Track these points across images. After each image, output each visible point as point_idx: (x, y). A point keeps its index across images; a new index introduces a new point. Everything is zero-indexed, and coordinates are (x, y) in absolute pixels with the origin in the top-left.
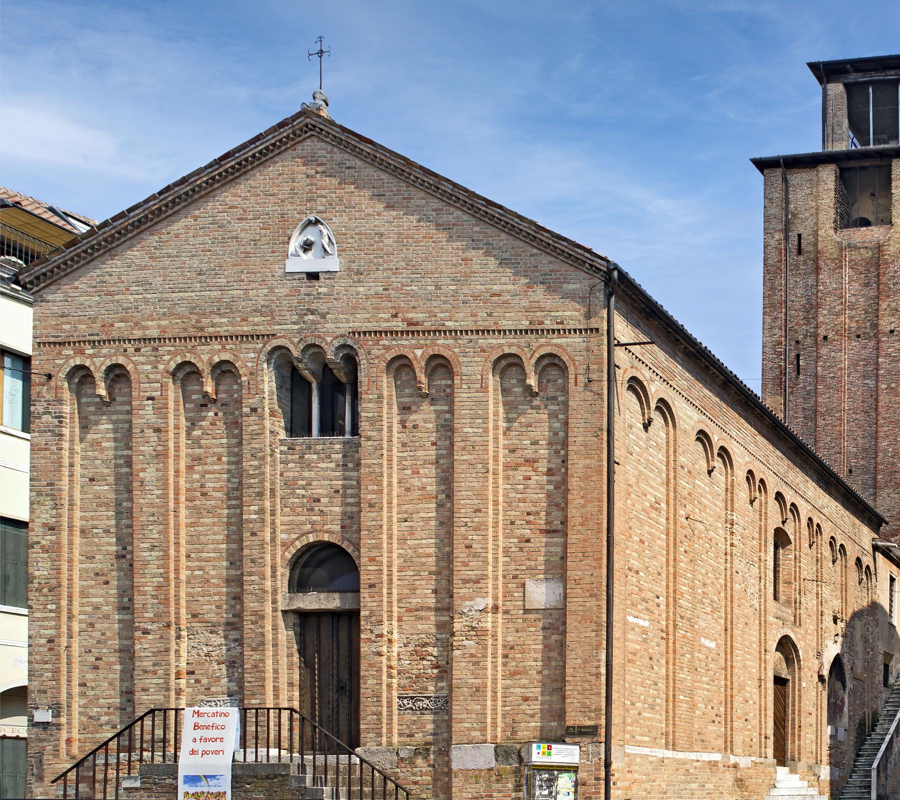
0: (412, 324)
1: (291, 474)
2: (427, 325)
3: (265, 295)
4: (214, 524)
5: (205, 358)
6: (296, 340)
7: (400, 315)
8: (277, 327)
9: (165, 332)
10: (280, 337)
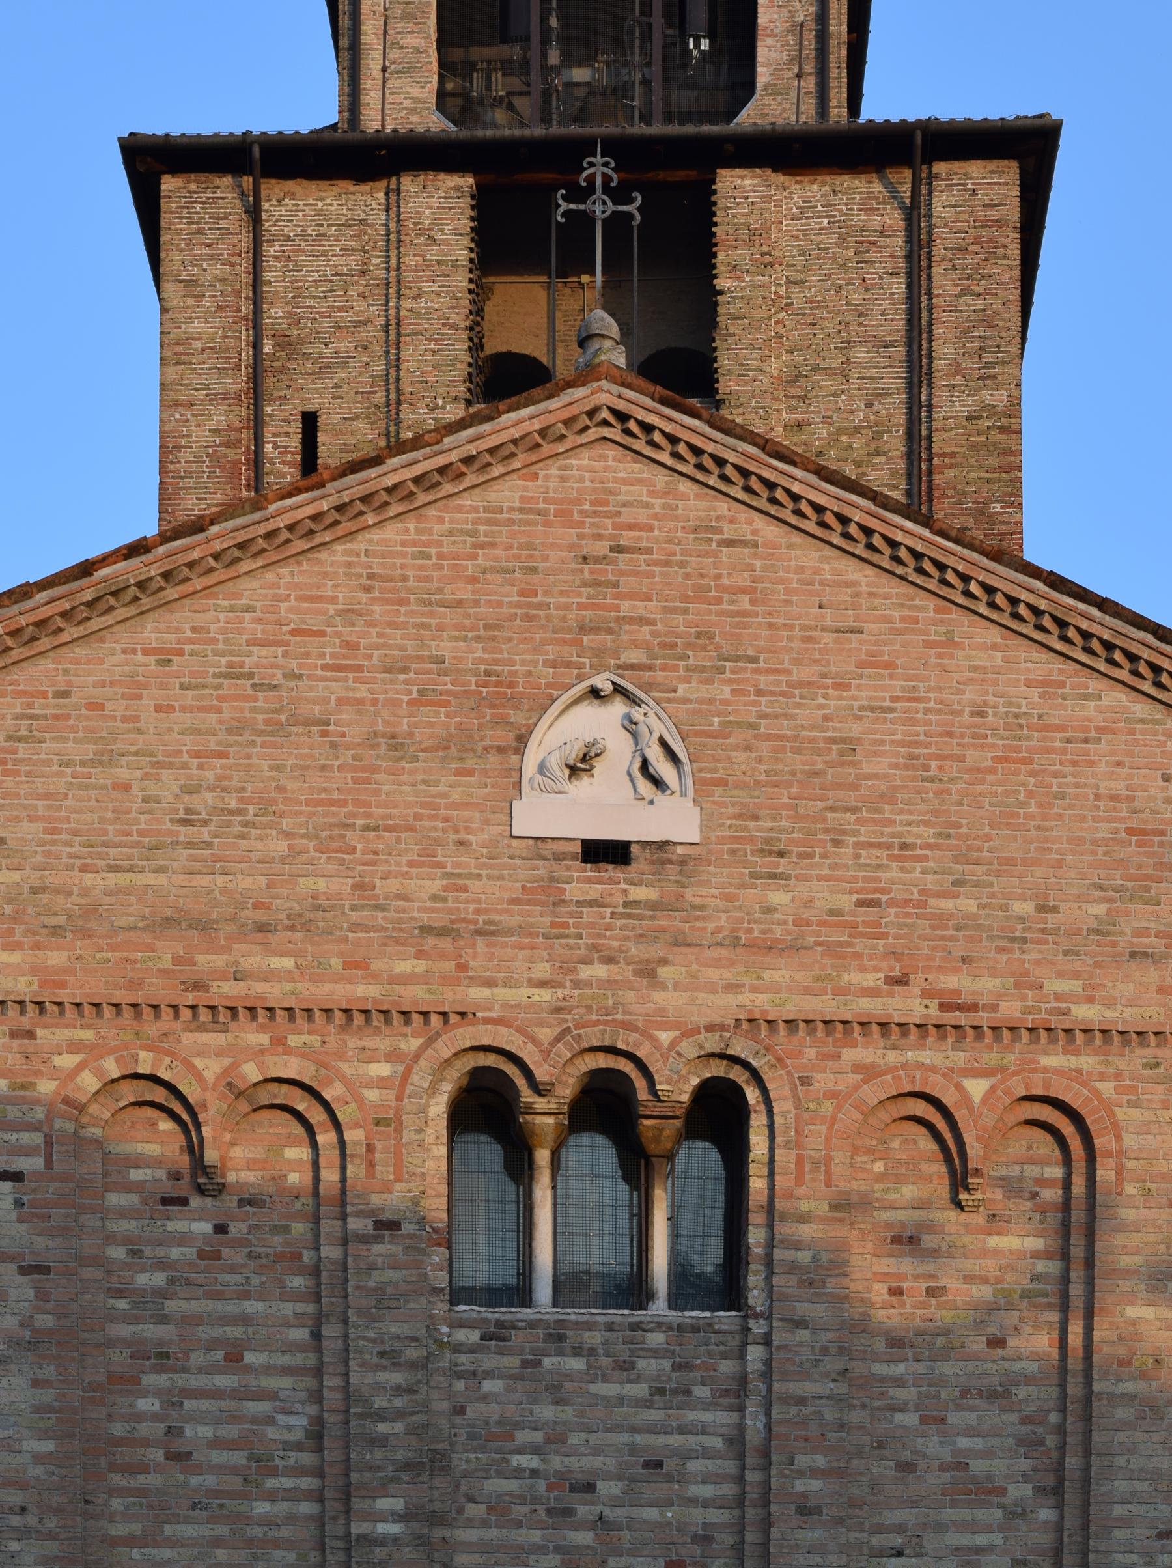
0: (959, 1008)
1: (493, 1411)
2: (1010, 1010)
3: (434, 898)
4: (217, 1543)
5: (211, 1068)
6: (545, 1034)
7: (916, 978)
8: (478, 994)
9: (63, 985)
10: (487, 1021)
